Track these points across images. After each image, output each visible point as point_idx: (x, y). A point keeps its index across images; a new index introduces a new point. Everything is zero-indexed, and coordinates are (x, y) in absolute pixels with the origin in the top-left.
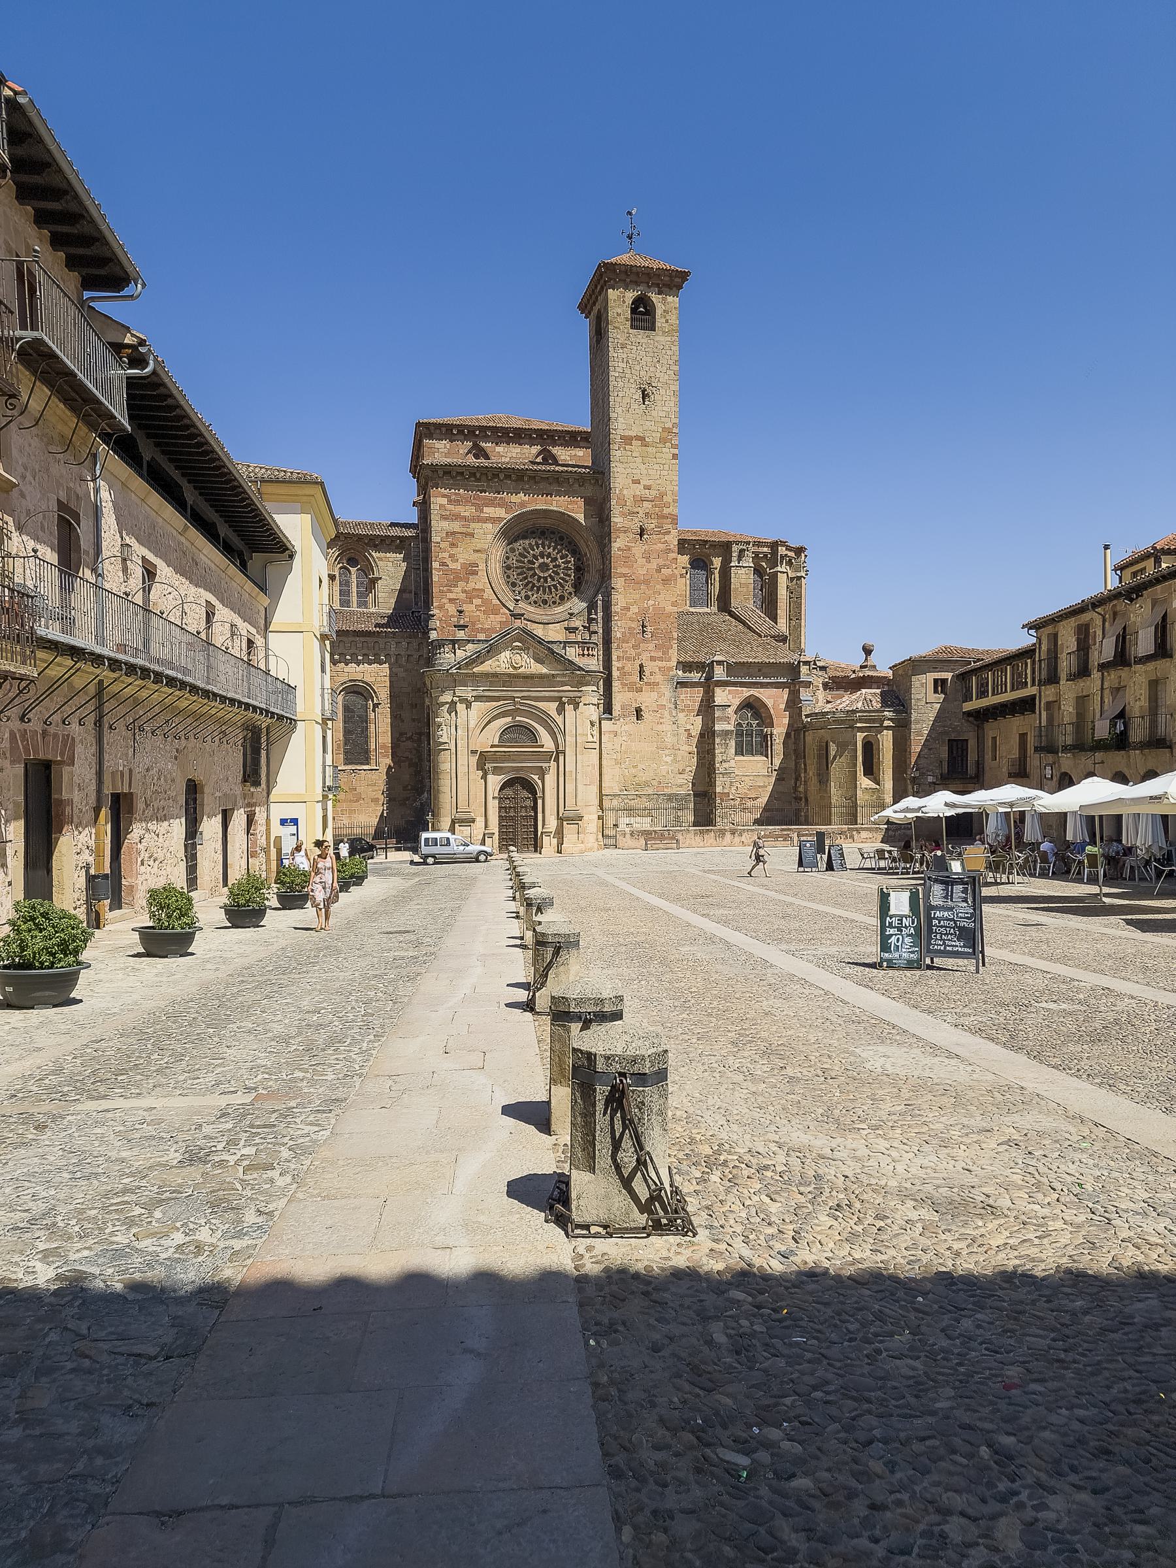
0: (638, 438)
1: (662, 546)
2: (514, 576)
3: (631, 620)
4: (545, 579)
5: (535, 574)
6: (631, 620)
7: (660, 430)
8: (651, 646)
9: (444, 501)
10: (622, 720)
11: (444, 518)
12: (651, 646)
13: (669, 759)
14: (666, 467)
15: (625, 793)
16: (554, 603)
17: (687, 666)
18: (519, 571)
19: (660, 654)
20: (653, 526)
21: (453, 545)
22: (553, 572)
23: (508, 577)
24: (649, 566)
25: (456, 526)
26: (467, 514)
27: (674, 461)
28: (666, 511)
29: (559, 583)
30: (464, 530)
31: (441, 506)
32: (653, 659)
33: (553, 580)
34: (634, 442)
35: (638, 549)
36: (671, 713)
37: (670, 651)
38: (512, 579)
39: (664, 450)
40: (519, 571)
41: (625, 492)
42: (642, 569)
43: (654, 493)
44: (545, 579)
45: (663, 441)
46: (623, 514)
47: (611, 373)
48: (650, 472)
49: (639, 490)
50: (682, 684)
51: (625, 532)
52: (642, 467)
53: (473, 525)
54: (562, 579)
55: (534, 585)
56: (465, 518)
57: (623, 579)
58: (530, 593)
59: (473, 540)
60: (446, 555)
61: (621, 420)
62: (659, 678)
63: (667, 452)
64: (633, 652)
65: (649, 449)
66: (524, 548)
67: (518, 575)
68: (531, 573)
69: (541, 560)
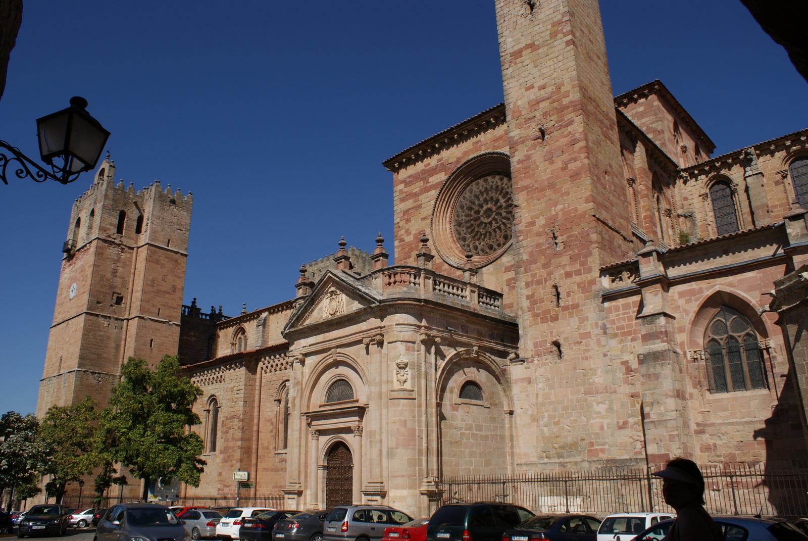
0: (528, 46)
1: (564, 141)
2: (463, 230)
3: (539, 234)
4: (490, 223)
5: (482, 223)
6: (539, 234)
7: (549, 27)
8: (565, 259)
9: (401, 186)
10: (536, 362)
11: (402, 200)
12: (565, 259)
13: (602, 408)
14: (560, 58)
15: (546, 460)
16: (499, 245)
17: (614, 272)
18: (468, 225)
19: (577, 266)
20: (552, 123)
21: (408, 221)
22: (497, 214)
23: (459, 234)
24: (554, 167)
25: (410, 203)
26: (417, 190)
27: (569, 48)
28: (565, 101)
29: (504, 224)
30: (415, 205)
31: (401, 191)
32: (568, 275)
33: (497, 223)
34: (524, 53)
35: (538, 154)
36: (598, 342)
37: (590, 259)
38: (462, 235)
39: (555, 43)
40: (468, 225)
41: (519, 103)
42: (544, 172)
43: (549, 90)
44: (490, 223)
45: (554, 35)
46: (519, 126)
47: (497, 7)
48: (544, 71)
49: (533, 95)
50: (608, 297)
51: (523, 142)
52: (535, 70)
53: (421, 197)
54: (505, 218)
55: (481, 234)
56: (416, 195)
57: (525, 192)
58: (477, 243)
59: (422, 210)
60: (403, 232)
61: (509, 40)
62: (578, 297)
63: (560, 43)
64: (543, 272)
65: (540, 51)
66: (471, 202)
67: (467, 228)
68: (478, 222)
69: (485, 207)
